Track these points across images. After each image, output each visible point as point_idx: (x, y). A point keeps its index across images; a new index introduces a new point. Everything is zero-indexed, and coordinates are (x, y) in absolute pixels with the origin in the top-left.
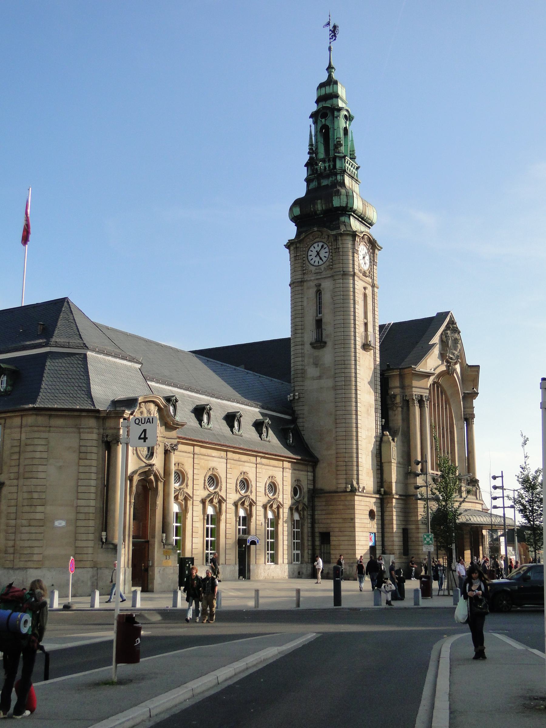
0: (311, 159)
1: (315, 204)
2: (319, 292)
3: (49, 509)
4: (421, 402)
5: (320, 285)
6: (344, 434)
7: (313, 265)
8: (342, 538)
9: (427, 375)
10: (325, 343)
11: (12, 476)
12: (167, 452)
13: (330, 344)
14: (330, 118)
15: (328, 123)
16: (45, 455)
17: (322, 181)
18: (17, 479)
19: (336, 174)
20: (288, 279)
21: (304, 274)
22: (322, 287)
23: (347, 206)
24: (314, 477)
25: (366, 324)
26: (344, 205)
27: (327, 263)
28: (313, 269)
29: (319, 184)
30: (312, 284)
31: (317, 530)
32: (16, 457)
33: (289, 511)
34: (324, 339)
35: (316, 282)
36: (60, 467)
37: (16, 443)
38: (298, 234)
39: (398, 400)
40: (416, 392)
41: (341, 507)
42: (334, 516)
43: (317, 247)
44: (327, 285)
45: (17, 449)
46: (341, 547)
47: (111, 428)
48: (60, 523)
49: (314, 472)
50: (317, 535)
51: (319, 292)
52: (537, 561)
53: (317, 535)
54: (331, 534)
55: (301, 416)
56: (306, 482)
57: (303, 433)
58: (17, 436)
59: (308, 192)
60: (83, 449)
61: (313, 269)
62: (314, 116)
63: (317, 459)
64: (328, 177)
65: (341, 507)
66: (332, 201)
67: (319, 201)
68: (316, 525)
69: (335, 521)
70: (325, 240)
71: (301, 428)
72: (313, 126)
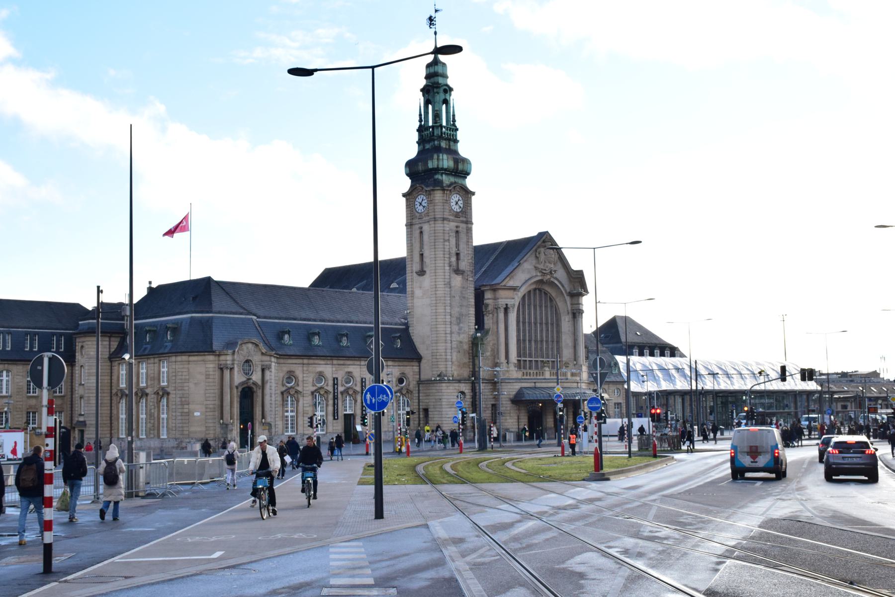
0: (420, 126)
1: (417, 165)
2: (421, 233)
3: (191, 407)
4: (506, 309)
5: (421, 228)
6: (435, 339)
7: (418, 212)
8: (436, 413)
9: (514, 289)
10: (425, 272)
11: (173, 388)
12: (263, 370)
13: (428, 272)
14: (432, 94)
15: (430, 98)
16: (187, 377)
17: (426, 145)
18: (175, 390)
19: (434, 140)
20: (404, 222)
21: (412, 219)
22: (423, 229)
23: (438, 167)
24: (420, 369)
25: (458, 255)
26: (436, 167)
27: (426, 212)
28: (417, 215)
29: (424, 147)
30: (417, 226)
31: (421, 407)
32: (174, 378)
33: (661, 343)
34: (425, 269)
35: (420, 225)
36: (196, 384)
37: (174, 370)
38: (411, 186)
39: (490, 308)
40: (502, 302)
41: (434, 391)
42: (431, 397)
43: (419, 199)
44: (426, 227)
45: (174, 374)
46: (435, 419)
47: (223, 360)
48: (197, 414)
49: (419, 366)
50: (421, 410)
51: (421, 233)
52: (501, 439)
53: (421, 410)
54: (429, 410)
55: (411, 325)
56: (412, 373)
57: (412, 338)
58: (174, 367)
59: (419, 153)
60: (208, 373)
61: (417, 214)
62: (422, 90)
63: (421, 356)
64: (429, 142)
65: (434, 391)
66: (428, 164)
67: (420, 164)
68: (421, 404)
69: (431, 400)
70: (424, 193)
71: (411, 334)
72: (422, 98)
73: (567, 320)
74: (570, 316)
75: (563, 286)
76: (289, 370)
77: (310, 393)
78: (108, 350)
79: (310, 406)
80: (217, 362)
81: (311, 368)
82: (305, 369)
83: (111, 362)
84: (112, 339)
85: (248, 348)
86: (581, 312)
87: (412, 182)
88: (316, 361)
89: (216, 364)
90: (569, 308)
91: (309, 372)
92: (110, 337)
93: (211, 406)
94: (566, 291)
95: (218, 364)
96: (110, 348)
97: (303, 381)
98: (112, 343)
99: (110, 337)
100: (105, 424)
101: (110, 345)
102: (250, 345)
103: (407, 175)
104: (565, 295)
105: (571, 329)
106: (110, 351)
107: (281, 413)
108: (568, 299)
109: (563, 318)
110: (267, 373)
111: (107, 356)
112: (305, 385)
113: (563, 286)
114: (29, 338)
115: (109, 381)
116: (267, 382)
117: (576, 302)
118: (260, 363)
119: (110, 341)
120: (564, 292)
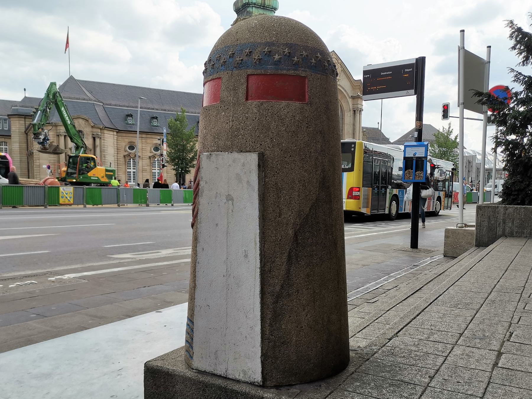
73: (349, 115)
74: (352, 112)
75: (345, 91)
76: (130, 141)
77: (148, 157)
78: (24, 127)
79: (148, 166)
80: (55, 131)
81: (149, 141)
82: (144, 141)
83: (27, 134)
84: (27, 120)
85: (78, 122)
86: (361, 110)
87: (238, 16)
88: (153, 136)
89: (54, 132)
90: (351, 107)
91: (147, 143)
92: (25, 118)
93: (52, 161)
94: (348, 96)
95: (56, 132)
96: (25, 125)
97: (142, 148)
98: (26, 122)
99: (25, 118)
100: (24, 174)
101: (25, 124)
102: (81, 121)
103: (234, 11)
104: (348, 98)
105: (352, 122)
106: (25, 128)
107: (124, 169)
108: (350, 101)
109: (346, 114)
110: (98, 141)
111: (24, 131)
112: (143, 152)
113: (345, 91)
114: (7, 122)
115: (26, 147)
116: (97, 147)
117: (356, 103)
118: (92, 133)
119: (25, 121)
120: (346, 95)
